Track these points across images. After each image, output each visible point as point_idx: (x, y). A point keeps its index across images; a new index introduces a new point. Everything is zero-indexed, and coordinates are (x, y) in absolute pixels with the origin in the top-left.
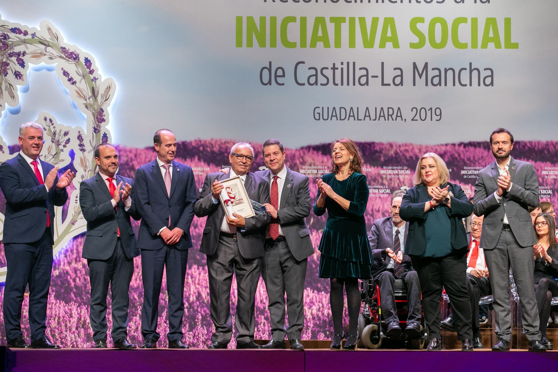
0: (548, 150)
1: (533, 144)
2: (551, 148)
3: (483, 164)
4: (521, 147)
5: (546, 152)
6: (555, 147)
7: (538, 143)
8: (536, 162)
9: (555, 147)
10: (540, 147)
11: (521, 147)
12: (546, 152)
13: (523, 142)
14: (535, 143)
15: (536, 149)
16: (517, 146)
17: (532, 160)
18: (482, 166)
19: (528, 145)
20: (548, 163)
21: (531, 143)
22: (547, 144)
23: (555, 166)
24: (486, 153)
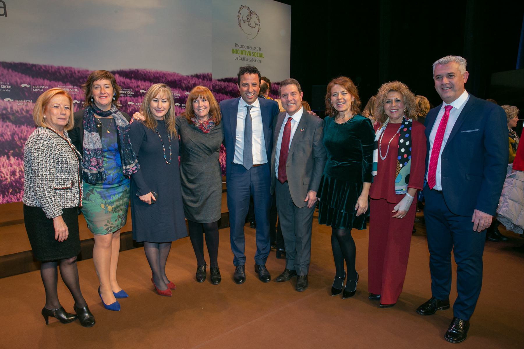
0: (60, 73)
1: (47, 68)
2: (62, 72)
3: (4, 80)
4: (37, 69)
5: (58, 74)
6: (65, 71)
7: (52, 67)
8: (50, 81)
9: (65, 71)
10: (53, 70)
11: (37, 69)
12: (58, 74)
13: (39, 65)
14: (49, 67)
15: (50, 71)
16: (34, 68)
17: (48, 79)
18: (3, 82)
19: (43, 68)
20: (60, 83)
21: (45, 66)
22: (59, 68)
23: (65, 85)
24: (5, 71)
